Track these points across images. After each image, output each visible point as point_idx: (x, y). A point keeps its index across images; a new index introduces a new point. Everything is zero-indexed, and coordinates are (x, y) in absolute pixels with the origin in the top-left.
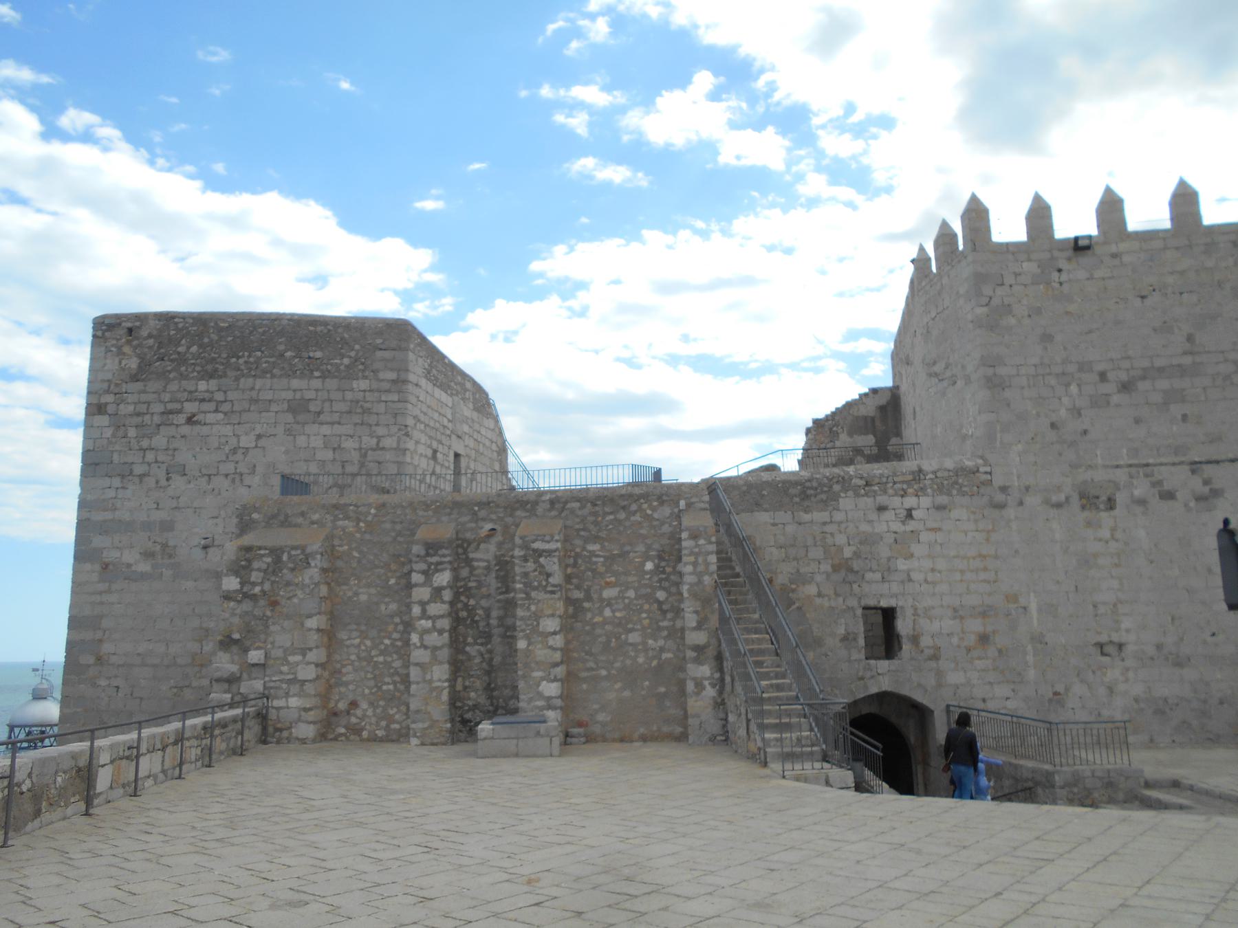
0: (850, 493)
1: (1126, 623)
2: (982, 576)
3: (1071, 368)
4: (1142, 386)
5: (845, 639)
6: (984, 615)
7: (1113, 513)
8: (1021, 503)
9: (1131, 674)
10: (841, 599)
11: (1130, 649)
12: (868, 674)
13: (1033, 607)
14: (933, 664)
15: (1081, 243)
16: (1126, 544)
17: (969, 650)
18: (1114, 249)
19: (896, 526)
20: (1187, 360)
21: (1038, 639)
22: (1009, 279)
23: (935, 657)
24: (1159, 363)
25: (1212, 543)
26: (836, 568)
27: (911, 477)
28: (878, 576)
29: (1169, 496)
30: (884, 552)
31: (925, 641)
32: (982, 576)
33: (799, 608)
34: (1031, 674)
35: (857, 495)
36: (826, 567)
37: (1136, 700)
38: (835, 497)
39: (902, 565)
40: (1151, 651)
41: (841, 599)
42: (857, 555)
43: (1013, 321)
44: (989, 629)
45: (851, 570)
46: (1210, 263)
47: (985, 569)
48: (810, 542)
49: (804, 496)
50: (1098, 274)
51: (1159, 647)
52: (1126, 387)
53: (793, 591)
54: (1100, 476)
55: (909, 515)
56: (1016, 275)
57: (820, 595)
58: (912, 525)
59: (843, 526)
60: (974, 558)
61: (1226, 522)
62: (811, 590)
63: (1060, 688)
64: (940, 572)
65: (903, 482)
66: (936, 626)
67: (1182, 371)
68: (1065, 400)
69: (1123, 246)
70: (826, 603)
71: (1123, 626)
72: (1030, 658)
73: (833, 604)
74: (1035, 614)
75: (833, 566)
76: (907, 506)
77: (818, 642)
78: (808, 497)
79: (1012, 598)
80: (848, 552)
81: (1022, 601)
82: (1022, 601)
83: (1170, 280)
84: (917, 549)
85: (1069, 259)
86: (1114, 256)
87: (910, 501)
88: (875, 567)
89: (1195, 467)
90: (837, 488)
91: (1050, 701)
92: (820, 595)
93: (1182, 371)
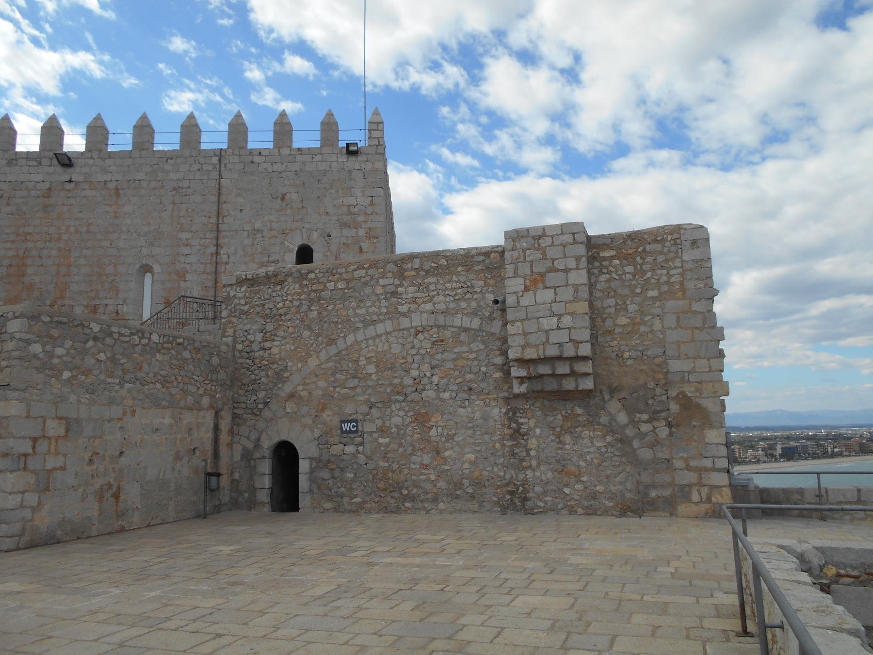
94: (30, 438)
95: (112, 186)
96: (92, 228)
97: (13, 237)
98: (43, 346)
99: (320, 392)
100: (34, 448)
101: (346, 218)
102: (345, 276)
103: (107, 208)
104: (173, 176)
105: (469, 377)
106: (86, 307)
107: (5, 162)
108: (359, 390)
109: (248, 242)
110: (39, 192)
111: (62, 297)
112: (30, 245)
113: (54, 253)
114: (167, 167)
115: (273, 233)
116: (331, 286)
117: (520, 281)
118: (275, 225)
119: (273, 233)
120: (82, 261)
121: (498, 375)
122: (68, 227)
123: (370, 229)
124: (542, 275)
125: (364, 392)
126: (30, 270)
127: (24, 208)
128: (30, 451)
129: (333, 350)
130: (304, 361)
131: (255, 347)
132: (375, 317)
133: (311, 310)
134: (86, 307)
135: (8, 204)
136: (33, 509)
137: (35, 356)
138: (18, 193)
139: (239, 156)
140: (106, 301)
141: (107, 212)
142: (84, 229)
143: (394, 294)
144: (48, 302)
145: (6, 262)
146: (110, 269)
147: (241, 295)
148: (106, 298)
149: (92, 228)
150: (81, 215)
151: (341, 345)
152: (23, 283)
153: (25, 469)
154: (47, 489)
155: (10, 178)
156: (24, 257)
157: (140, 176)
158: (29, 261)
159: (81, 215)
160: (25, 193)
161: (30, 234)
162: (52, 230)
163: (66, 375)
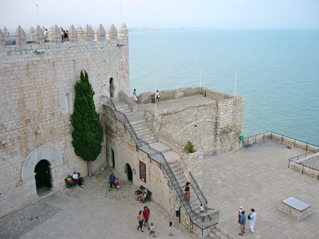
95: (51, 61)
96: (47, 81)
97: (17, 90)
99: (180, 140)
101: (121, 67)
102: (186, 112)
103: (51, 72)
104: (72, 55)
105: (209, 131)
106: (50, 114)
107: (6, 53)
108: (188, 138)
109: (97, 79)
110: (24, 67)
111: (41, 112)
112: (25, 92)
113: (35, 94)
114: (70, 51)
115: (103, 75)
116: (183, 114)
117: (223, 112)
118: (104, 72)
119: (103, 75)
120: (46, 96)
121: (214, 130)
122: (38, 82)
123: (127, 70)
124: (226, 111)
125: (189, 138)
126: (27, 104)
127: (19, 76)
129: (183, 129)
130: (176, 133)
131: (164, 131)
132: (192, 121)
133: (178, 121)
134: (50, 114)
135: (12, 75)
138: (15, 69)
139: (92, 45)
140: (58, 110)
141: (52, 73)
142: (45, 82)
143: (196, 115)
144: (36, 116)
145: (17, 102)
146: (56, 98)
147: (160, 118)
148: (57, 109)
149: (47, 81)
150: (42, 76)
151: (185, 128)
152: (25, 110)
155: (10, 62)
156: (24, 99)
157: (61, 56)
158: (26, 100)
159: (42, 76)
160: (18, 68)
161: (24, 87)
162: (32, 84)
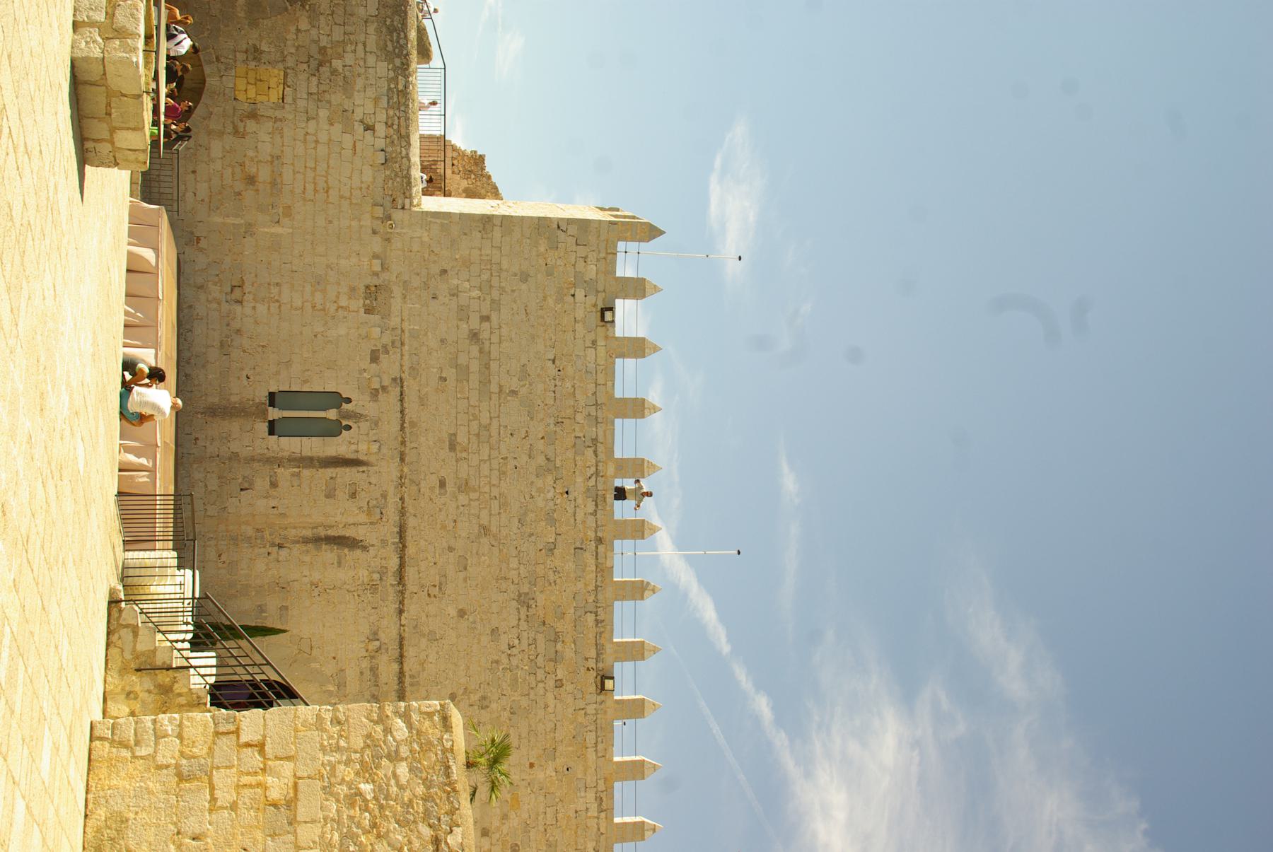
0: (392, 74)
1: (262, 308)
2: (310, 187)
3: (495, 294)
4: (475, 350)
5: (256, 49)
6: (274, 183)
7: (362, 310)
8: (374, 232)
9: (215, 305)
10: (293, 50)
11: (238, 308)
12: (223, 67)
13: (278, 230)
14: (230, 129)
15: (608, 315)
16: (333, 317)
17: (242, 165)
18: (601, 342)
19: (359, 114)
20: (494, 388)
21: (249, 229)
22: (582, 251)
23: (236, 132)
24: (494, 366)
25: (330, 388)
26: (322, 50)
27: (403, 133)
28: (314, 90)
29: (374, 358)
30: (337, 98)
31: (251, 125)
32: (310, 187)
33: (286, 9)
34: (217, 219)
35: (389, 81)
36: (324, 41)
37: (191, 307)
38: (389, 59)
39: (323, 113)
40: (236, 325)
41: (293, 50)
42: (334, 72)
43: (542, 249)
44: (261, 187)
45: (321, 64)
46: (579, 417)
47: (316, 191)
48: (349, 29)
49: (392, 29)
50: (579, 327)
51: (238, 331)
52: (474, 336)
53: (303, 6)
54: (396, 304)
55: (368, 128)
56: (585, 259)
57: (298, 31)
58: (359, 129)
59: (362, 63)
60: (326, 182)
61: (349, 400)
62: (304, 25)
63: (203, 244)
64: (315, 148)
65: (399, 125)
66: (264, 136)
67: (485, 382)
68: (467, 285)
69: (602, 351)
70: (291, 36)
71: (258, 305)
72: (230, 220)
73: (289, 43)
74: (273, 230)
75: (325, 48)
76: (377, 126)
77: (254, 24)
78: (391, 33)
79: (288, 211)
80: (337, 64)
81: (285, 221)
82: (285, 221)
83: (569, 385)
84: (338, 127)
85: (595, 305)
86: (594, 342)
87: (381, 129)
88: (322, 88)
89: (399, 381)
90: (398, 62)
91: (192, 233)
92: (298, 31)
93: (485, 382)
94: (264, 737)
98: (408, 742)
100: (248, 745)
128: (244, 739)
136: (153, 757)
137: (388, 731)
153: (217, 734)
154: (181, 777)
163: (366, 788)
